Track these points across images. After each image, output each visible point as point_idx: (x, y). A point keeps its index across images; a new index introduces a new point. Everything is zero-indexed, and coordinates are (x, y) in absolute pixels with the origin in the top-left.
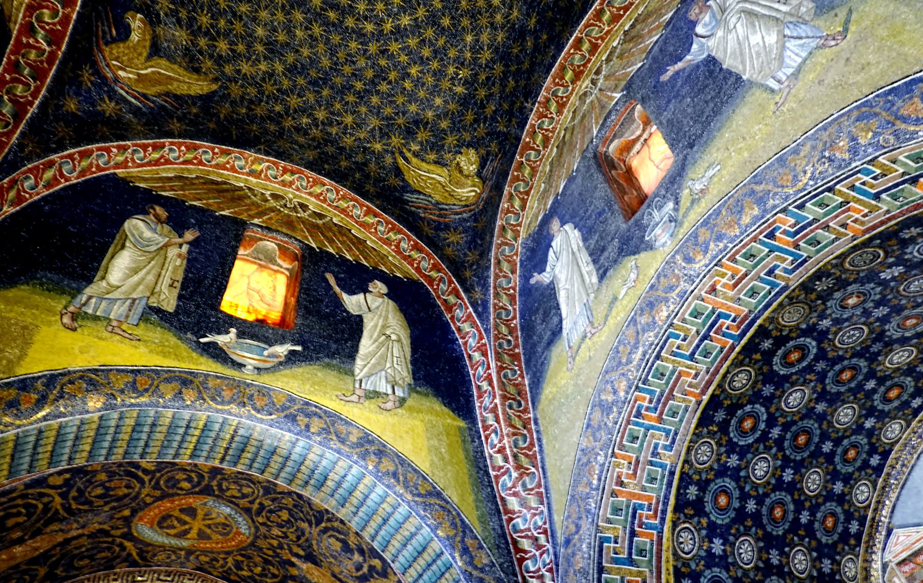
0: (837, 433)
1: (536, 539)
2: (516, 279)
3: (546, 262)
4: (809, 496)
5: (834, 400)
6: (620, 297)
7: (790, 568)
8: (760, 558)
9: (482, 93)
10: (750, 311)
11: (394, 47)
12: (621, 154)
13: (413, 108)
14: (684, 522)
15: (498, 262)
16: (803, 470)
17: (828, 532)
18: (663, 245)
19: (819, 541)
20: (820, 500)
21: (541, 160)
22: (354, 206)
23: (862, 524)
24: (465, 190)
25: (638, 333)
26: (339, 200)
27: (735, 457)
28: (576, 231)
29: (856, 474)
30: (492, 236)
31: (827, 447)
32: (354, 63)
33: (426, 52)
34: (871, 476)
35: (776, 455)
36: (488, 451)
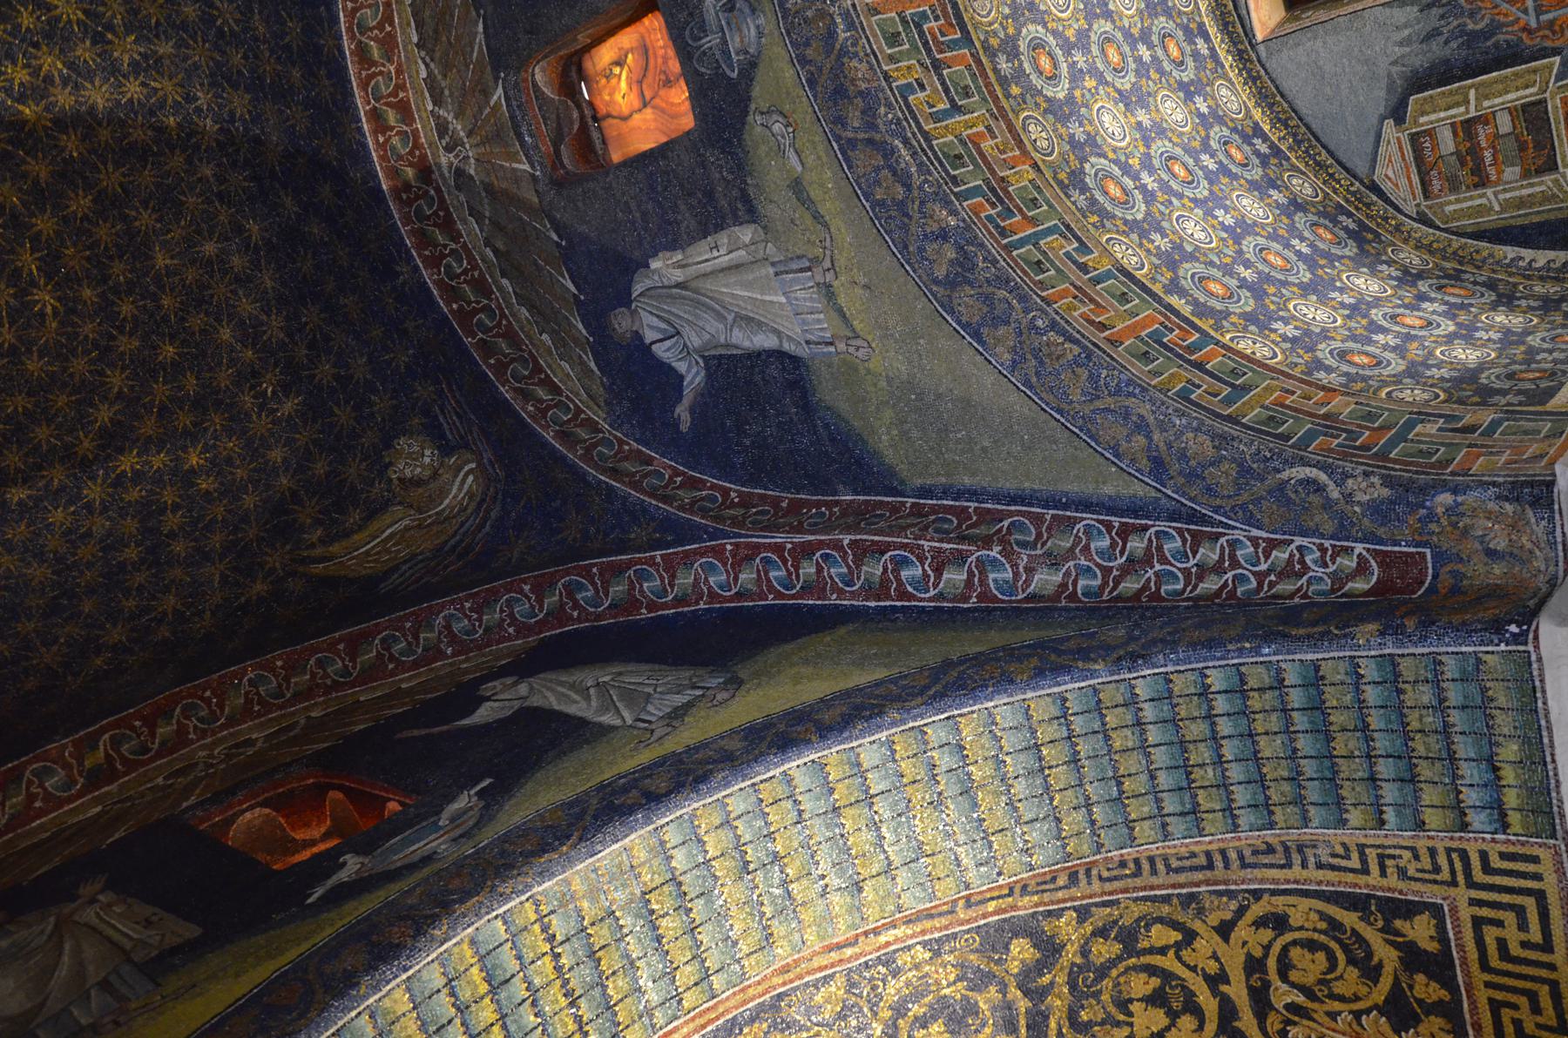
1: (1130, 560)
2: (663, 463)
3: (671, 369)
6: (799, 169)
9: (326, 368)
11: (128, 463)
12: (588, 162)
13: (249, 501)
15: (615, 473)
18: (760, 34)
19: (1349, 258)
20: (1286, 221)
21: (503, 315)
22: (320, 663)
24: (454, 491)
25: (870, 141)
26: (287, 679)
28: (655, 264)
30: (564, 458)
32: (89, 534)
33: (185, 420)
36: (926, 599)
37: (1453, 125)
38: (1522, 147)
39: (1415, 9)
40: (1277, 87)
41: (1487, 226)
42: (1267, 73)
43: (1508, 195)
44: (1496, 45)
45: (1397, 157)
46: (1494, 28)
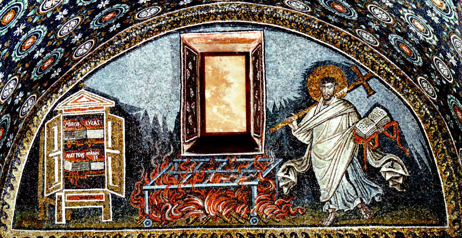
37: (103, 139)
38: (80, 173)
40: (151, 41)
41: (41, 147)
43: (56, 162)
44: (140, 168)
45: (93, 105)
46: (149, 169)
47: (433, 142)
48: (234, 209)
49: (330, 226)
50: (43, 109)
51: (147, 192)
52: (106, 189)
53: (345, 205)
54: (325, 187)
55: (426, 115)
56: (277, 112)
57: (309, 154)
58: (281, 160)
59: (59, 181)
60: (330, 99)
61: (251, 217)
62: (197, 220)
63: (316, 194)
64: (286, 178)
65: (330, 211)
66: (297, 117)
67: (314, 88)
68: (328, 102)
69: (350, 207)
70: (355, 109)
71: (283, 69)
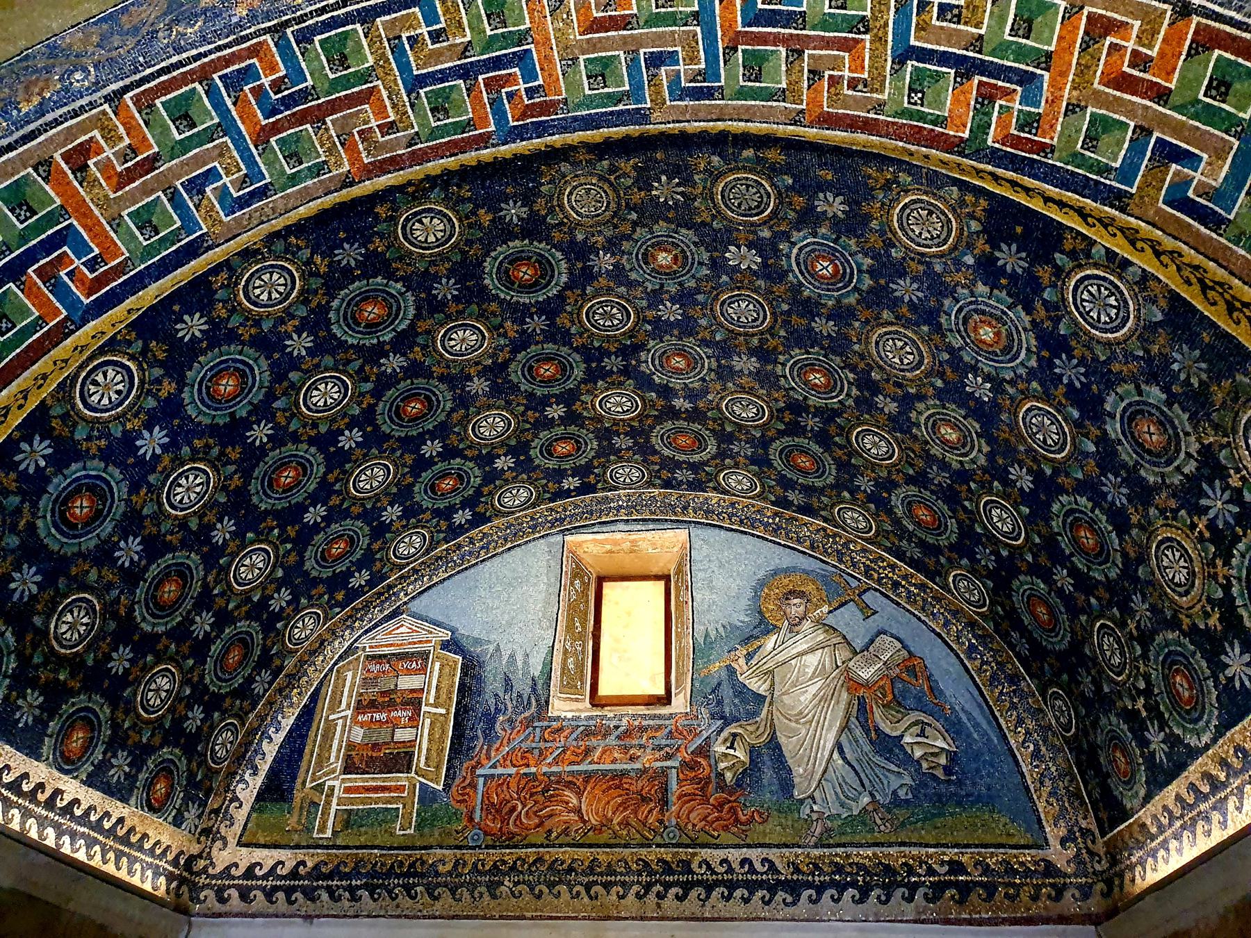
0: (461, 441)
4: (348, 493)
5: (502, 389)
7: (230, 565)
8: (200, 515)
10: (565, 102)
14: (132, 357)
16: (375, 451)
17: (324, 558)
19: (301, 562)
20: (356, 510)
23: (371, 584)
27: (306, 341)
29: (428, 515)
31: (431, 448)
34: (438, 532)
35: (362, 394)
38: (375, 746)
39: (537, 674)
42: (534, 539)
47: (992, 692)
48: (635, 812)
49: (816, 846)
50: (336, 643)
51: (481, 780)
52: (413, 774)
53: (842, 805)
54: (801, 771)
55: (971, 645)
56: (711, 643)
57: (770, 712)
58: (720, 722)
59: (336, 761)
60: (800, 623)
61: (666, 827)
62: (566, 832)
63: (786, 785)
64: (730, 756)
65: (815, 816)
66: (745, 652)
67: (771, 607)
68: (796, 629)
69: (851, 810)
70: (844, 637)
71: (719, 581)
